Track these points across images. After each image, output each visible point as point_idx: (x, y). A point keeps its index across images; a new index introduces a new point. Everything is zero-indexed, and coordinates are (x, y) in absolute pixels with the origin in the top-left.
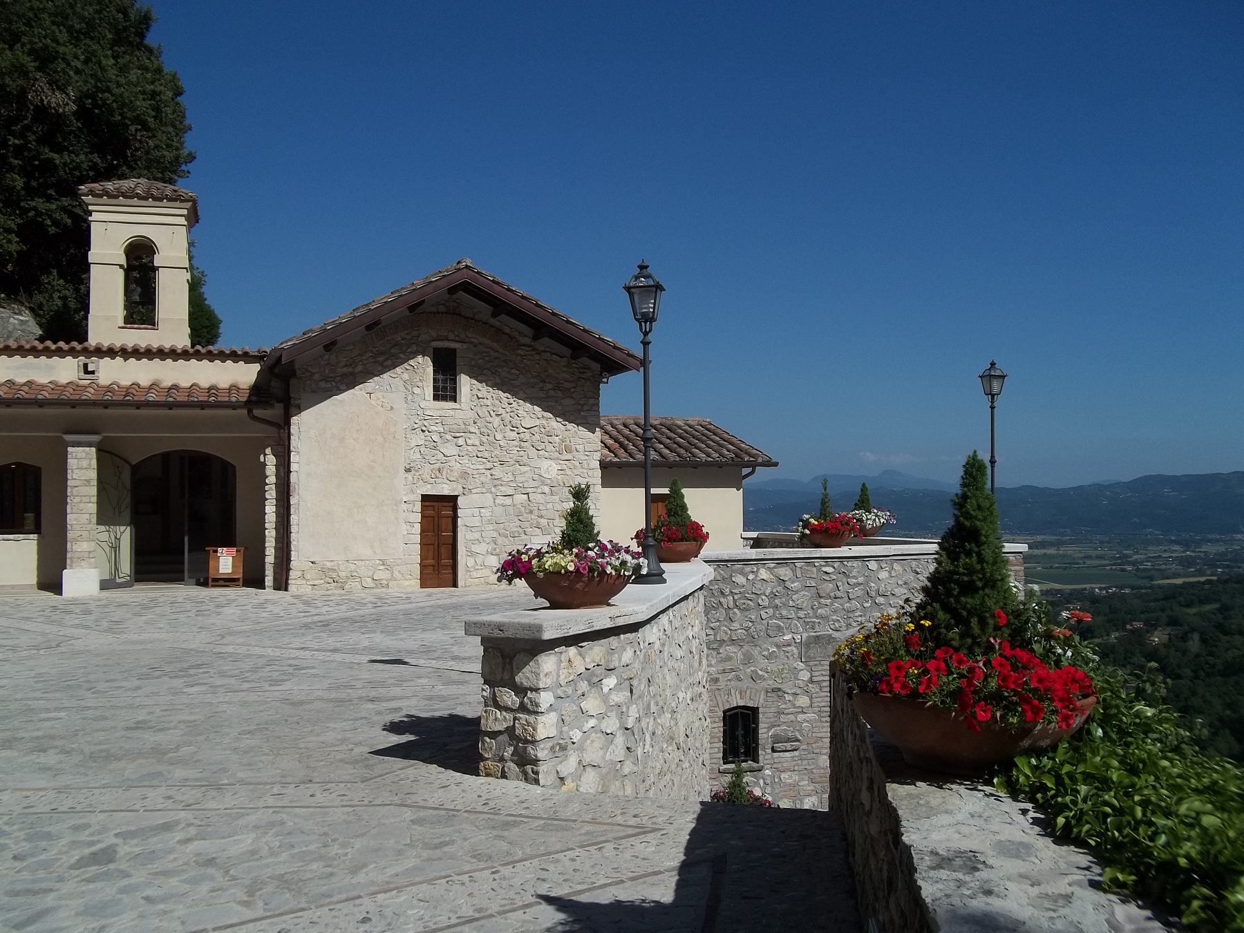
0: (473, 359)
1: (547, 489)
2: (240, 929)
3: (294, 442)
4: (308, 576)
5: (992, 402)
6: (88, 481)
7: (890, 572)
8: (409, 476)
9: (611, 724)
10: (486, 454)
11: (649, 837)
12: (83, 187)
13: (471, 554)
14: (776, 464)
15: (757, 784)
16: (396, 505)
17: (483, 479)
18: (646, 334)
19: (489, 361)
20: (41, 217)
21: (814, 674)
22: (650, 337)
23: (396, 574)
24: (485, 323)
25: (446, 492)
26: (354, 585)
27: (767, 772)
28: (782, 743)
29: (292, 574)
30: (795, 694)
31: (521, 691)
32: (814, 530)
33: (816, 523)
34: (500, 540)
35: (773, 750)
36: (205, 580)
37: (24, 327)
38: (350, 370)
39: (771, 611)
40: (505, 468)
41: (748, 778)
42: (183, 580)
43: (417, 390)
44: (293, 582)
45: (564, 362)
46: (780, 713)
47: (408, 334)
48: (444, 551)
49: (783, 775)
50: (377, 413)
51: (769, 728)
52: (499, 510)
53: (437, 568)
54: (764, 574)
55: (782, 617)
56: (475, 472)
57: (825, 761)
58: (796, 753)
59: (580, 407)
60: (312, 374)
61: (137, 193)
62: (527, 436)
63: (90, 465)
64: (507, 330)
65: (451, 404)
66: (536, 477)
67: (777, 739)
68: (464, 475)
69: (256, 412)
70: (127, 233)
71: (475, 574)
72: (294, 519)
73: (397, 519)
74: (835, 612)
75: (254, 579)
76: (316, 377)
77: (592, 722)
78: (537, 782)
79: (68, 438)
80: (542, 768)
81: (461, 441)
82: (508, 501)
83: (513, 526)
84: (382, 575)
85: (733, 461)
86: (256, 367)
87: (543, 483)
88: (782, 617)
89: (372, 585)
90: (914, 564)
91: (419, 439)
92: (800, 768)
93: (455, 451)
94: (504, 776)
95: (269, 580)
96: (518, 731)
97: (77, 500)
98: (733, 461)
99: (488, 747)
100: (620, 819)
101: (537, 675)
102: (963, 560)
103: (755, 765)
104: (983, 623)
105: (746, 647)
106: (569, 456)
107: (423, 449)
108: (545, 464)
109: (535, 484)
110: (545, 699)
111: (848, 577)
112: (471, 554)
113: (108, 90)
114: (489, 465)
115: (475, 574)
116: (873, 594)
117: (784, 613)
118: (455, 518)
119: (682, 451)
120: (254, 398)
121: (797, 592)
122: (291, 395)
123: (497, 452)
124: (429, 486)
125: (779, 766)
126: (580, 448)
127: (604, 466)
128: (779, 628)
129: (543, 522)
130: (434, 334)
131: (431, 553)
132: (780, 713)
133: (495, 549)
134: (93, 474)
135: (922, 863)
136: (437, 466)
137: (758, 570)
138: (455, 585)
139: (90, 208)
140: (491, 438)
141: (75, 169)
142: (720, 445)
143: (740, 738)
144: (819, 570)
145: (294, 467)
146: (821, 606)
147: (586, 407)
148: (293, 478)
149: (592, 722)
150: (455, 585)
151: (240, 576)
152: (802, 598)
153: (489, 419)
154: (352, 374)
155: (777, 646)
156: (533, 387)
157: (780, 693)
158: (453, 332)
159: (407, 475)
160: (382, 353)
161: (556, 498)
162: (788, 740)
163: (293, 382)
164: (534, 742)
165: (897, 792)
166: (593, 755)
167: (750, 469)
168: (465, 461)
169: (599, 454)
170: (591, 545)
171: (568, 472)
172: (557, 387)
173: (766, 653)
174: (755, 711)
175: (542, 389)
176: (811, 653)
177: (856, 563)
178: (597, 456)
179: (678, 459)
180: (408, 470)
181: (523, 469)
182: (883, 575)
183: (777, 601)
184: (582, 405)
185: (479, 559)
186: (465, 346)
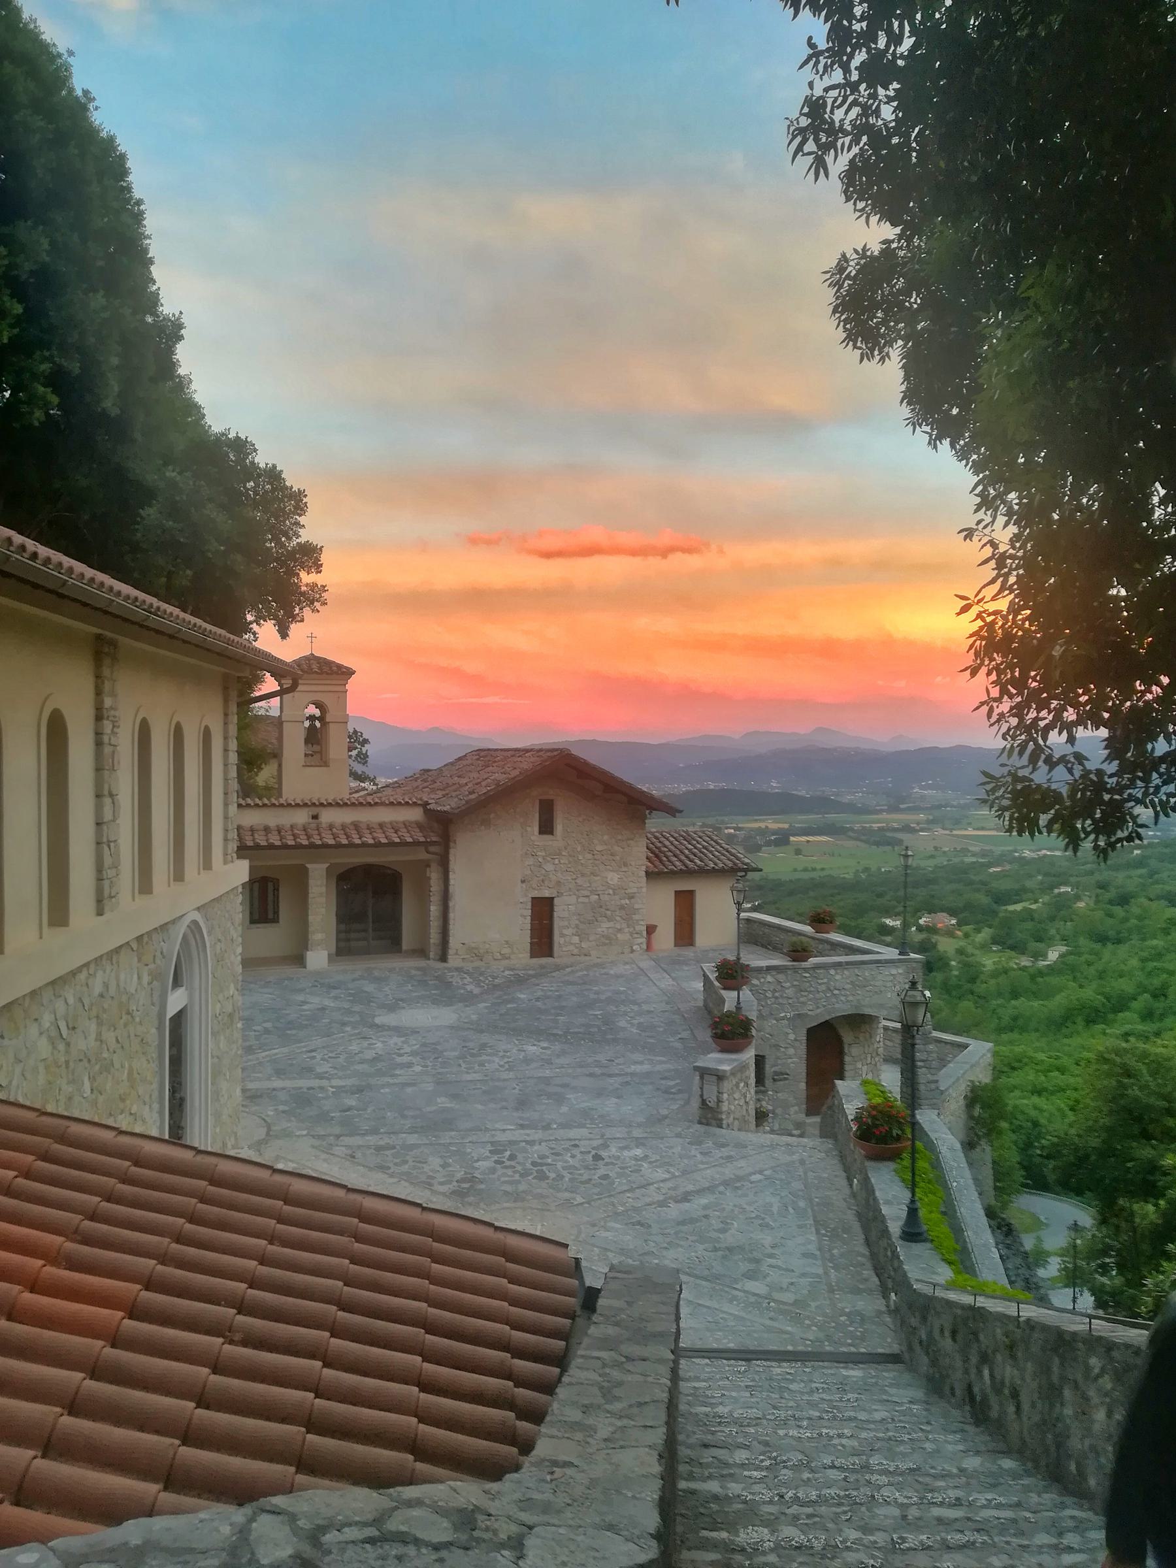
2: (369, 1186)
3: (452, 865)
8: (524, 885)
9: (742, 1102)
10: (572, 870)
13: (562, 935)
25: (547, 895)
27: (770, 1093)
28: (780, 1076)
29: (451, 952)
30: (786, 1048)
35: (774, 1080)
39: (773, 1000)
43: (529, 829)
46: (778, 1058)
49: (779, 1095)
54: (769, 979)
55: (778, 1004)
57: (803, 1086)
65: (550, 837)
67: (776, 1073)
68: (559, 883)
71: (564, 949)
72: (451, 915)
74: (810, 1000)
80: (724, 1122)
81: (557, 861)
82: (586, 900)
84: (506, 951)
87: (609, 888)
89: (500, 957)
90: (856, 971)
91: (530, 861)
95: (432, 955)
103: (762, 1088)
112: (562, 935)
114: (574, 877)
118: (552, 910)
121: (788, 988)
123: (580, 867)
126: (633, 863)
127: (646, 872)
134: (324, 889)
138: (550, 954)
145: (452, 882)
146: (802, 996)
148: (451, 889)
149: (737, 1102)
150: (550, 954)
152: (790, 992)
161: (617, 897)
166: (737, 1117)
167: (743, 874)
168: (559, 874)
178: (644, 868)
180: (523, 882)
181: (596, 878)
182: (838, 977)
183: (777, 994)
185: (567, 939)
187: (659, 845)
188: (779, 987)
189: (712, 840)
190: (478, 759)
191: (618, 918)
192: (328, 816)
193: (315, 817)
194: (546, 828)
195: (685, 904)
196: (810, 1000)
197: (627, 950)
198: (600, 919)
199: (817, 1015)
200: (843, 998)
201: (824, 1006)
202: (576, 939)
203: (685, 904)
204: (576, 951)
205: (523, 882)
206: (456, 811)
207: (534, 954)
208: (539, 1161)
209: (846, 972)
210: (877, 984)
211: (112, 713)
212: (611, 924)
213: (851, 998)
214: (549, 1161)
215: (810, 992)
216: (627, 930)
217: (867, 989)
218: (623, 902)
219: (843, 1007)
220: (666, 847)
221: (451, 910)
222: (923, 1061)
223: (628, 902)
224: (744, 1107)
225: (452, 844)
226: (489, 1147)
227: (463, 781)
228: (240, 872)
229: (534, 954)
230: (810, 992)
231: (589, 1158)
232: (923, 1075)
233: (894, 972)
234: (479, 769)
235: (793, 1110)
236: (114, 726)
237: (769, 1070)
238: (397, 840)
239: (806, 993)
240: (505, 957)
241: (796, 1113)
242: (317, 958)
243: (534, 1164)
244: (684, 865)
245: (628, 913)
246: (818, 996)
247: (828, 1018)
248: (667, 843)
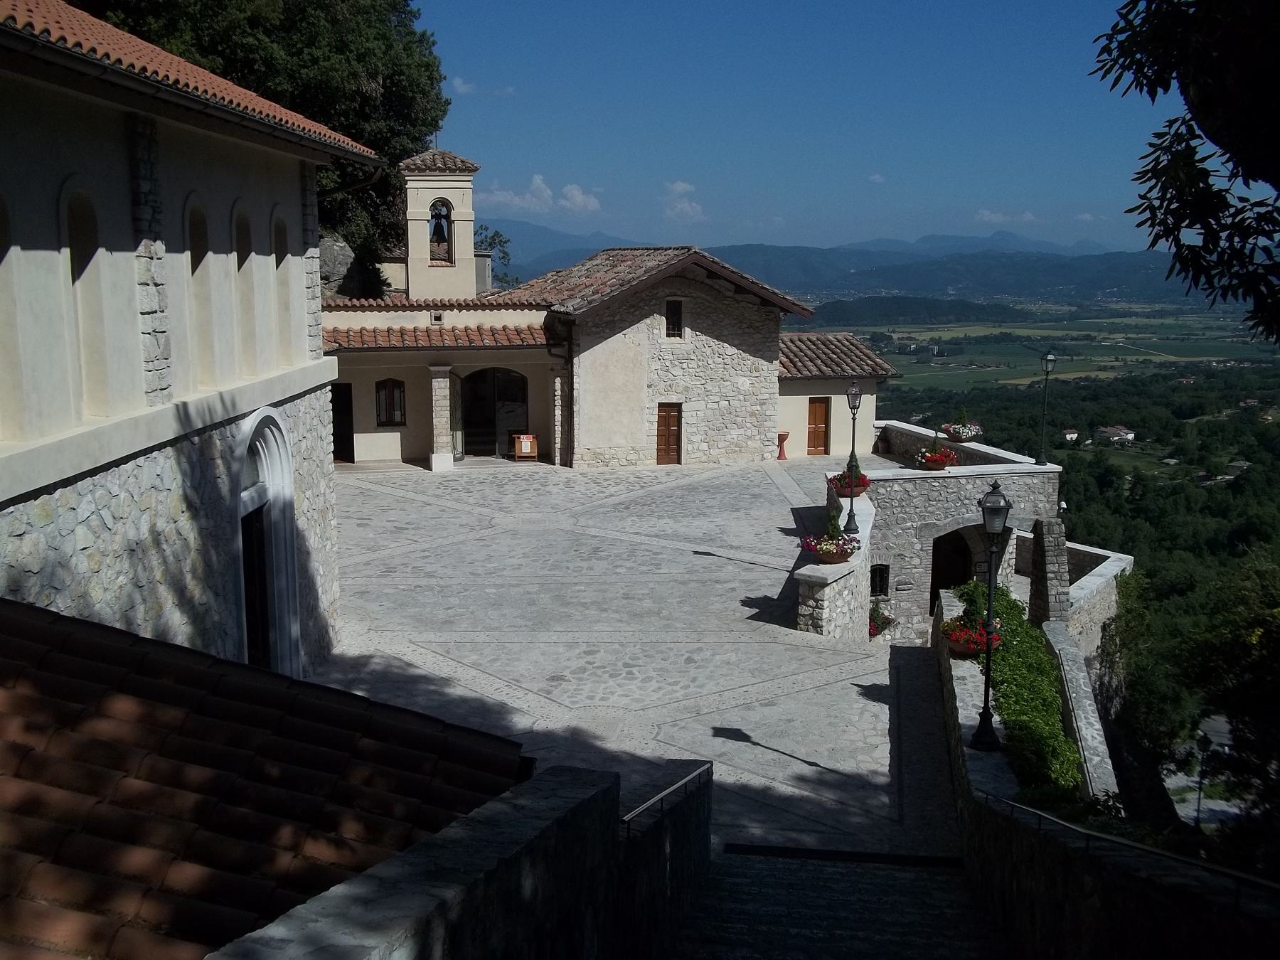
0: (694, 308)
1: (741, 397)
4: (585, 458)
6: (445, 396)
7: (973, 485)
9: (845, 610)
10: (702, 374)
11: (872, 658)
12: (402, 164)
15: (886, 609)
16: (642, 410)
17: (699, 391)
18: (854, 414)
19: (704, 309)
20: (356, 171)
21: (924, 546)
23: (641, 456)
24: (702, 283)
26: (614, 463)
28: (903, 585)
31: (817, 601)
32: (928, 460)
33: (930, 455)
34: (710, 432)
35: (897, 590)
36: (511, 455)
37: (343, 252)
38: (612, 319)
40: (714, 383)
41: (882, 605)
42: (495, 454)
44: (576, 462)
45: (755, 308)
46: (902, 568)
47: (650, 292)
48: (672, 439)
49: (902, 604)
50: (629, 348)
51: (895, 577)
52: (709, 412)
53: (667, 451)
55: (906, 513)
56: (694, 386)
58: (910, 591)
59: (766, 340)
60: (587, 323)
61: (439, 167)
62: (729, 361)
63: (446, 386)
64: (717, 287)
66: (735, 389)
67: (899, 583)
68: (687, 389)
69: (554, 351)
70: (431, 196)
71: (693, 456)
73: (642, 419)
74: (938, 509)
75: (545, 455)
76: (590, 324)
77: (839, 610)
78: (822, 634)
79: (432, 368)
80: (824, 629)
81: (685, 366)
82: (715, 406)
83: (719, 423)
85: (870, 374)
86: (544, 313)
88: (906, 513)
91: (656, 365)
92: (913, 599)
93: (680, 372)
94: (808, 631)
95: (558, 460)
96: (815, 615)
97: (439, 409)
98: (870, 374)
99: (801, 620)
100: (859, 651)
101: (824, 595)
102: (972, 607)
103: (886, 598)
104: (976, 623)
105: (884, 530)
106: (757, 374)
107: (659, 372)
108: (741, 380)
109: (734, 394)
110: (826, 604)
112: (690, 442)
113: (402, 73)
114: (703, 382)
115: (693, 456)
117: (908, 510)
118: (679, 418)
119: (835, 368)
120: (551, 342)
121: (915, 498)
122: (574, 337)
124: (663, 397)
125: (899, 598)
127: (781, 379)
128: (904, 519)
129: (739, 419)
130: (667, 291)
131: (663, 443)
132: (902, 568)
133: (706, 439)
134: (448, 392)
135: (954, 678)
136: (668, 383)
137: (893, 485)
138: (679, 462)
139: (406, 178)
140: (705, 363)
141: (378, 133)
142: (861, 360)
143: (878, 583)
144: (930, 484)
145: (576, 386)
147: (770, 340)
149: (839, 610)
150: (679, 462)
151: (536, 454)
153: (703, 350)
154: (613, 321)
155: (902, 530)
156: (734, 326)
157: (902, 557)
158: (680, 290)
159: (649, 390)
160: (633, 306)
161: (748, 403)
162: (906, 584)
163: (574, 328)
164: (821, 620)
165: (952, 661)
168: (687, 379)
169: (778, 372)
170: (840, 538)
171: (756, 385)
172: (750, 326)
173: (895, 534)
174: (887, 567)
175: (740, 328)
176: (922, 534)
177: (952, 480)
178: (777, 373)
179: (832, 374)
180: (650, 386)
182: (969, 487)
184: (767, 338)
185: (696, 446)
186: (688, 299)
188: (905, 496)
189: (852, 344)
190: (608, 259)
191: (748, 425)
192: (452, 319)
193: (438, 318)
194: (674, 329)
195: (820, 414)
197: (757, 458)
198: (729, 425)
199: (945, 525)
202: (704, 446)
203: (820, 414)
204: (704, 458)
205: (650, 386)
206: (578, 312)
207: (660, 461)
208: (630, 662)
211: (151, 197)
212: (741, 431)
214: (640, 662)
216: (757, 438)
218: (754, 408)
220: (801, 351)
221: (575, 415)
222: (1053, 572)
223: (759, 408)
224: (848, 615)
225: (576, 348)
226: (584, 648)
227: (588, 281)
228: (329, 369)
229: (660, 461)
231: (682, 659)
232: (1054, 588)
234: (607, 268)
235: (916, 619)
236: (154, 212)
237: (892, 580)
238: (519, 342)
240: (630, 463)
241: (919, 622)
242: (443, 460)
243: (626, 665)
244: (820, 370)
245: (760, 420)
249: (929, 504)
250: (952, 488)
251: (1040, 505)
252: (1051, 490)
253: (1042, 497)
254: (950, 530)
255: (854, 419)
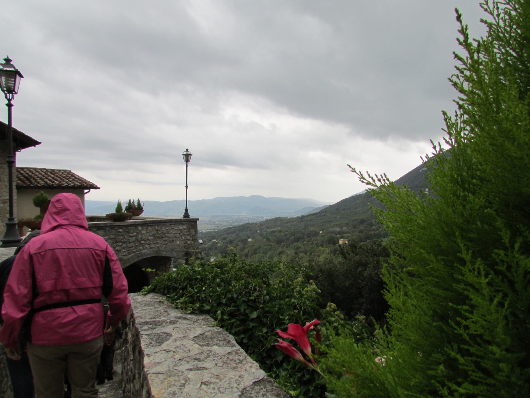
5: (187, 164)
14: (99, 188)
18: (9, 100)
22: (12, 102)
74: (124, 248)
90: (156, 227)
111: (129, 233)
116: (140, 239)
146: (118, 246)
167: (88, 190)
182: (143, 232)
187: (31, 174)
196: (124, 248)
199: (129, 259)
200: (148, 246)
201: (134, 252)
209: (150, 228)
210: (169, 235)
213: (153, 246)
215: (124, 242)
217: (163, 239)
219: (147, 251)
230: (124, 242)
233: (181, 228)
239: (120, 244)
246: (129, 245)
247: (137, 260)
248: (37, 174)
249: (117, 245)
250: (132, 233)
251: (188, 242)
252: (194, 233)
253: (189, 237)
254: (132, 262)
255: (10, 106)
